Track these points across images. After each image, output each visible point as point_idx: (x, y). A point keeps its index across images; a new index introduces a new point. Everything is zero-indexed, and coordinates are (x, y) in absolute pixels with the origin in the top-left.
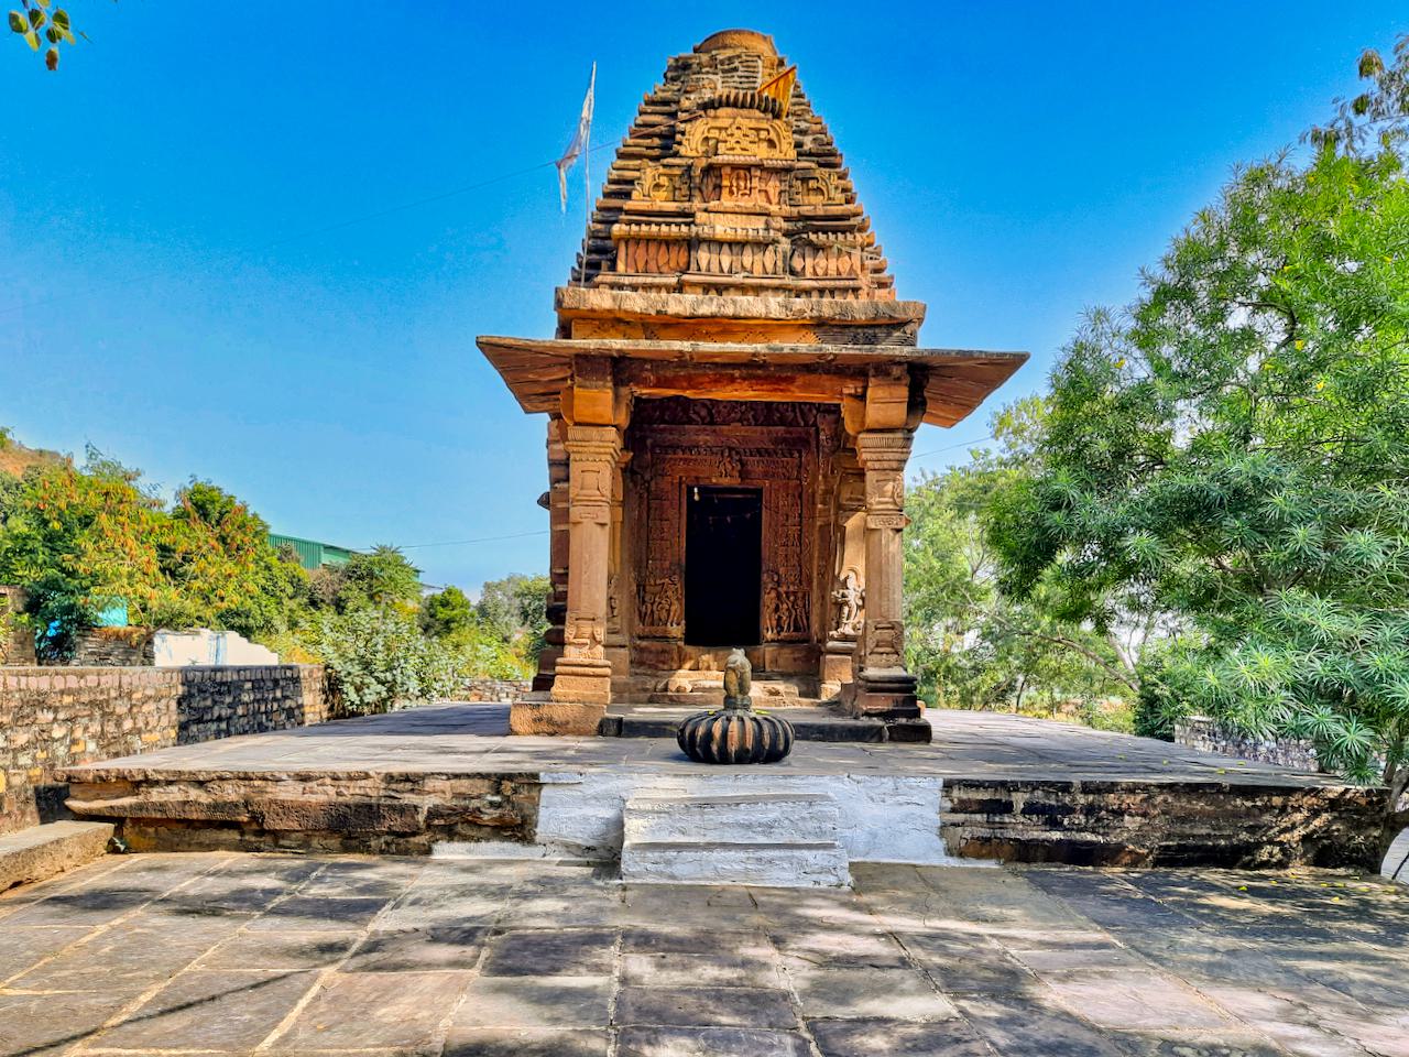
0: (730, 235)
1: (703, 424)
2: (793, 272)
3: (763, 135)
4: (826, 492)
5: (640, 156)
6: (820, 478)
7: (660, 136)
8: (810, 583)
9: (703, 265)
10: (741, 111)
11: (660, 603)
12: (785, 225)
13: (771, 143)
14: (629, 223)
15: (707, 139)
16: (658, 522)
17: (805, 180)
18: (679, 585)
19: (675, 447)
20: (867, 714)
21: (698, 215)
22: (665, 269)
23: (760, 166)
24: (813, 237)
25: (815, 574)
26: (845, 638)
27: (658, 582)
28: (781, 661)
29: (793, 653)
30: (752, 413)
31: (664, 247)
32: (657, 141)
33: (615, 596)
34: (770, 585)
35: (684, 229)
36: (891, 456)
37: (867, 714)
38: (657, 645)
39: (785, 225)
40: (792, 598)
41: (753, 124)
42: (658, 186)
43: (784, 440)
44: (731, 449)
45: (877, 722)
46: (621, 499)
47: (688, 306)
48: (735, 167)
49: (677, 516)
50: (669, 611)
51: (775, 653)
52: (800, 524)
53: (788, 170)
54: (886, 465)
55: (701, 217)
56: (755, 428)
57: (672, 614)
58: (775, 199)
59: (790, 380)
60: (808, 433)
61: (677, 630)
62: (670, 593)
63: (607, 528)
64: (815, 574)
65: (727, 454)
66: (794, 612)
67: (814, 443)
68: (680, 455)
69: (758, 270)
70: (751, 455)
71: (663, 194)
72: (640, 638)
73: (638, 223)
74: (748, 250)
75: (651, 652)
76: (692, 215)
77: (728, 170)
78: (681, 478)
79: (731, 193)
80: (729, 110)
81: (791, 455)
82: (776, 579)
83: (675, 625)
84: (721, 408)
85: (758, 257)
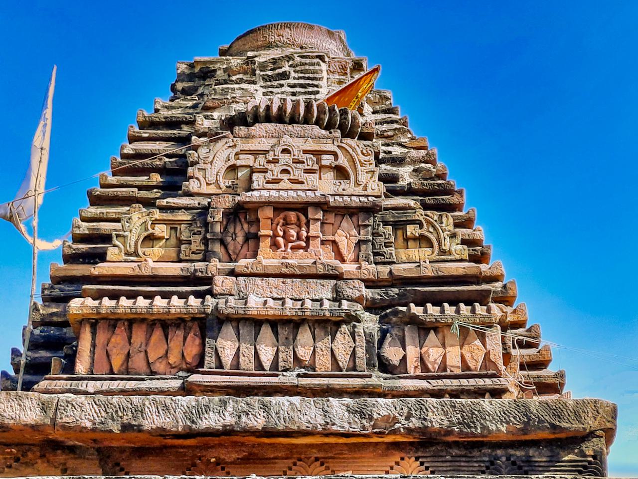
0: (273, 309)
2: (385, 367)
3: (327, 160)
5: (128, 201)
7: (162, 171)
9: (228, 357)
10: (290, 127)
12: (369, 293)
13: (341, 173)
14: (98, 296)
15: (233, 168)
17: (399, 225)
21: (219, 279)
22: (160, 367)
23: (322, 205)
24: (417, 310)
31: (158, 334)
32: (156, 178)
35: (193, 301)
39: (369, 293)
41: (311, 145)
42: (151, 239)
48: (280, 207)
53: (370, 210)
55: (222, 283)
58: (349, 254)
69: (323, 363)
71: (158, 250)
73: (114, 296)
74: (305, 336)
76: (209, 281)
77: (269, 212)
79: (275, 245)
80: (270, 127)
85: (324, 344)
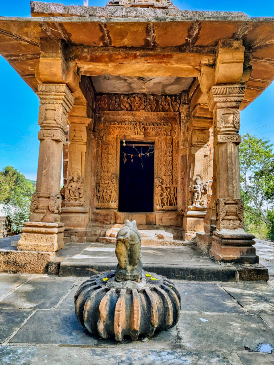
1: (127, 110)
4: (184, 140)
6: (182, 134)
8: (177, 183)
11: (106, 192)
16: (106, 155)
18: (115, 184)
19: (114, 121)
20: (224, 261)
25: (179, 178)
26: (197, 209)
27: (106, 182)
28: (164, 220)
29: (169, 216)
30: (150, 106)
33: (81, 188)
34: (158, 184)
36: (232, 99)
37: (224, 261)
38: (103, 212)
40: (169, 190)
43: (164, 118)
44: (140, 122)
45: (231, 267)
46: (86, 141)
47: (108, 12)
49: (115, 152)
50: (110, 196)
51: (161, 216)
52: (172, 156)
54: (229, 104)
56: (151, 112)
57: (112, 197)
59: (170, 57)
60: (175, 115)
61: (114, 205)
62: (111, 187)
63: (61, 144)
64: (179, 178)
65: (138, 125)
66: (170, 197)
67: (178, 120)
68: (117, 125)
70: (149, 125)
72: (97, 208)
75: (101, 215)
78: (117, 136)
81: (168, 125)
82: (161, 181)
83: (113, 203)
84: (135, 104)
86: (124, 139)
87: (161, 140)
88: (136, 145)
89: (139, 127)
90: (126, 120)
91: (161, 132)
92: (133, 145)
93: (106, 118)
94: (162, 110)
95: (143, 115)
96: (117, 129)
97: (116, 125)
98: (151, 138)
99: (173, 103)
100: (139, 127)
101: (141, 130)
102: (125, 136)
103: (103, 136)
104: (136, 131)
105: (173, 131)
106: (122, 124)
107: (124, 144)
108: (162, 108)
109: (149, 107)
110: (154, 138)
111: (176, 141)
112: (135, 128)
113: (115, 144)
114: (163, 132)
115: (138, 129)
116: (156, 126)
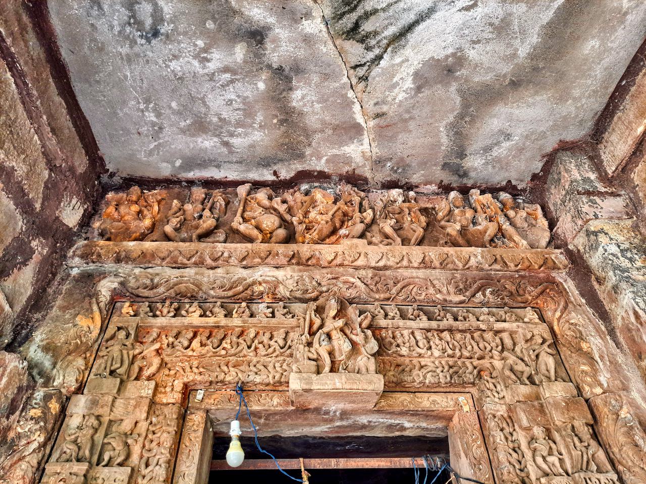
43: (487, 281)
56: (399, 249)
65: (333, 313)
68: (194, 318)
70: (403, 316)
78: (187, 391)
84: (313, 214)
86: (240, 417)
87: (502, 411)
88: (318, 464)
89: (340, 323)
90: (258, 289)
91: (485, 363)
92: (299, 464)
93: (132, 283)
94: (460, 240)
95: (360, 262)
96: (196, 344)
97: (186, 321)
98: (426, 401)
99: (511, 213)
100: (340, 323)
101: (353, 344)
102: (242, 389)
103: (80, 390)
104: (321, 348)
105: (565, 351)
106: (228, 315)
107: (235, 456)
108: (463, 231)
109: (387, 226)
110: (441, 402)
111: (623, 414)
112: (312, 334)
113: (162, 454)
114: (498, 364)
115: (336, 335)
116: (449, 321)
